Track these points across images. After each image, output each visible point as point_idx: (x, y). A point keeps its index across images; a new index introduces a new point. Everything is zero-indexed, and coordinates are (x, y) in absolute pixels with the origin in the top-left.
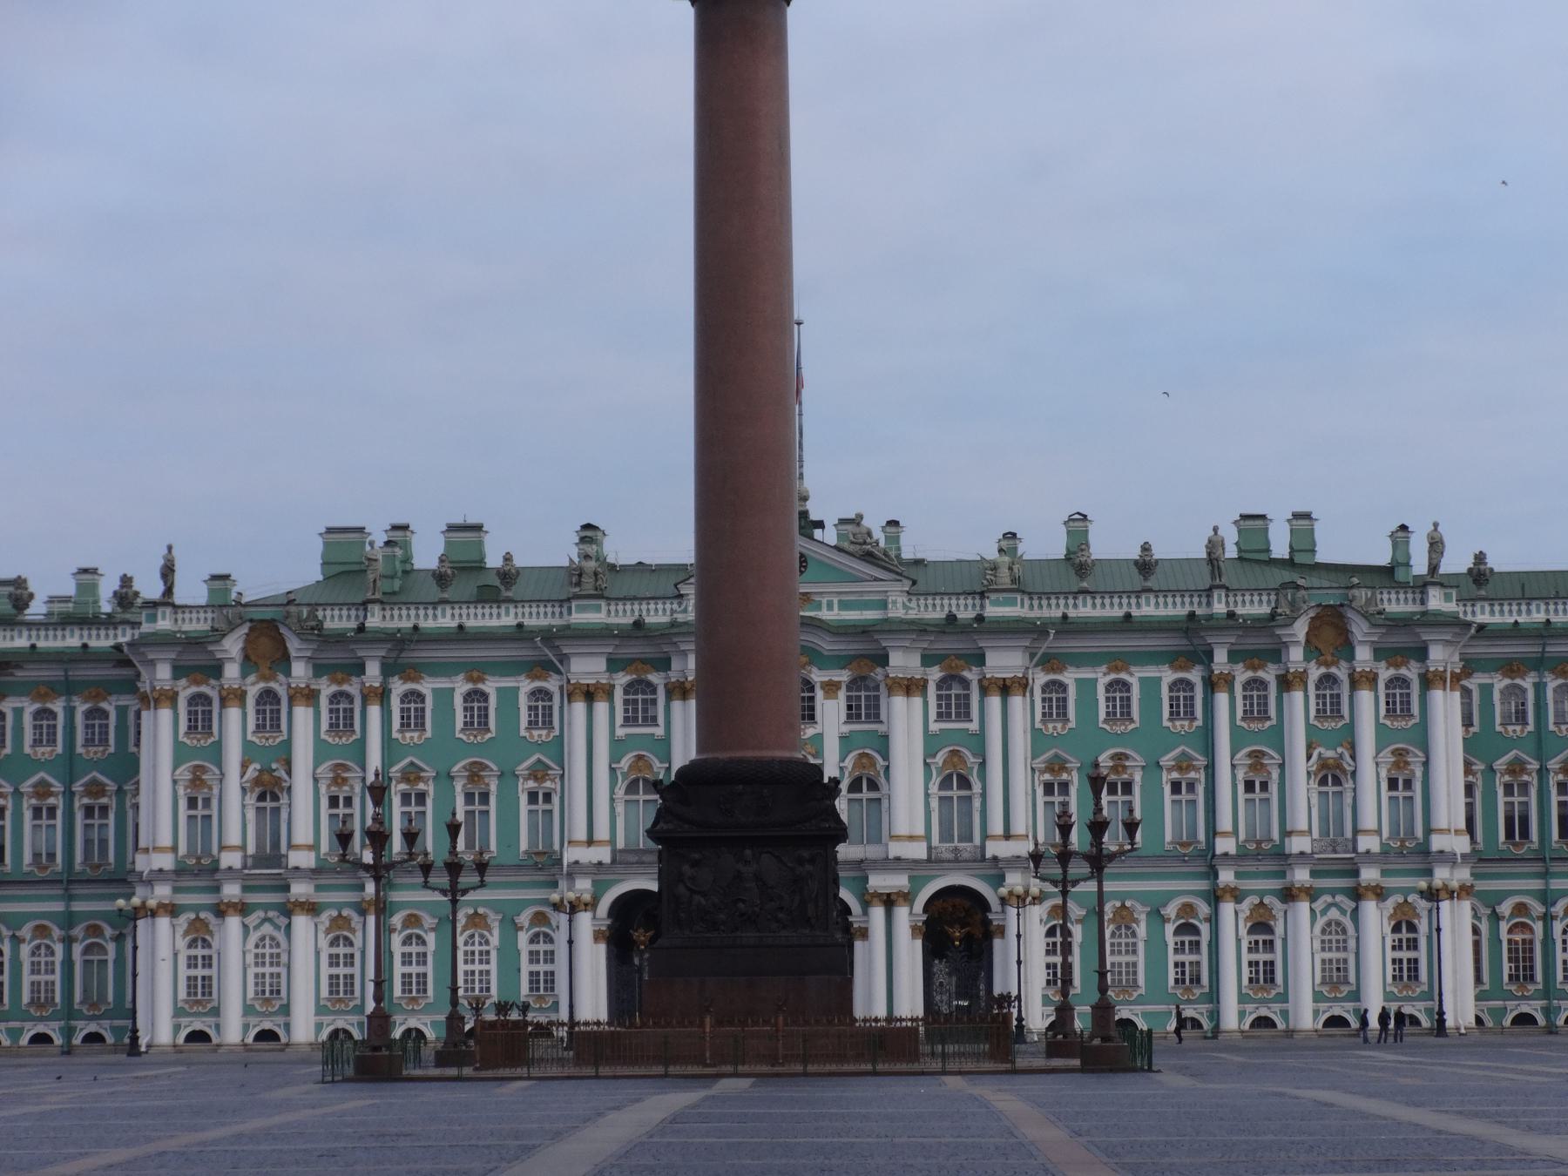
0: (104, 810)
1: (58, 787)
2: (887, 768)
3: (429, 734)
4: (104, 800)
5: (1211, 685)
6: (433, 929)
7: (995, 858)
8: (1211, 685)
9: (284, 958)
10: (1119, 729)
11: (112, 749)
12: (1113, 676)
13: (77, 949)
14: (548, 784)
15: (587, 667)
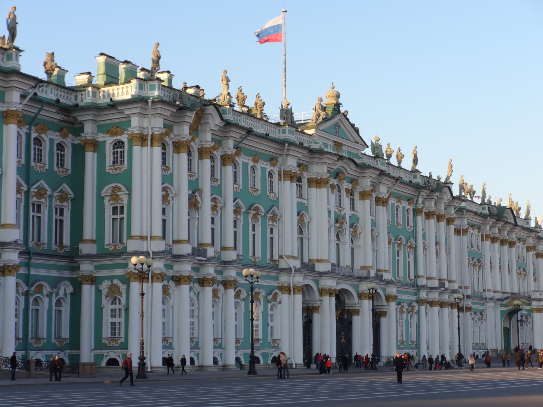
0: (39, 206)
1: (25, 188)
2: (360, 233)
3: (241, 188)
4: (43, 200)
5: (417, 212)
6: (243, 300)
7: (385, 280)
8: (417, 212)
9: (196, 313)
10: (399, 228)
11: (47, 167)
12: (398, 204)
13: (31, 299)
14: (275, 223)
15: (291, 163)
